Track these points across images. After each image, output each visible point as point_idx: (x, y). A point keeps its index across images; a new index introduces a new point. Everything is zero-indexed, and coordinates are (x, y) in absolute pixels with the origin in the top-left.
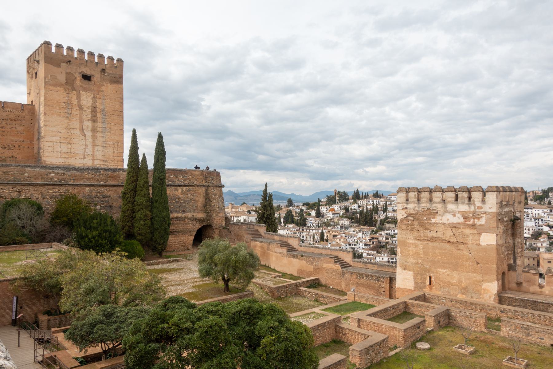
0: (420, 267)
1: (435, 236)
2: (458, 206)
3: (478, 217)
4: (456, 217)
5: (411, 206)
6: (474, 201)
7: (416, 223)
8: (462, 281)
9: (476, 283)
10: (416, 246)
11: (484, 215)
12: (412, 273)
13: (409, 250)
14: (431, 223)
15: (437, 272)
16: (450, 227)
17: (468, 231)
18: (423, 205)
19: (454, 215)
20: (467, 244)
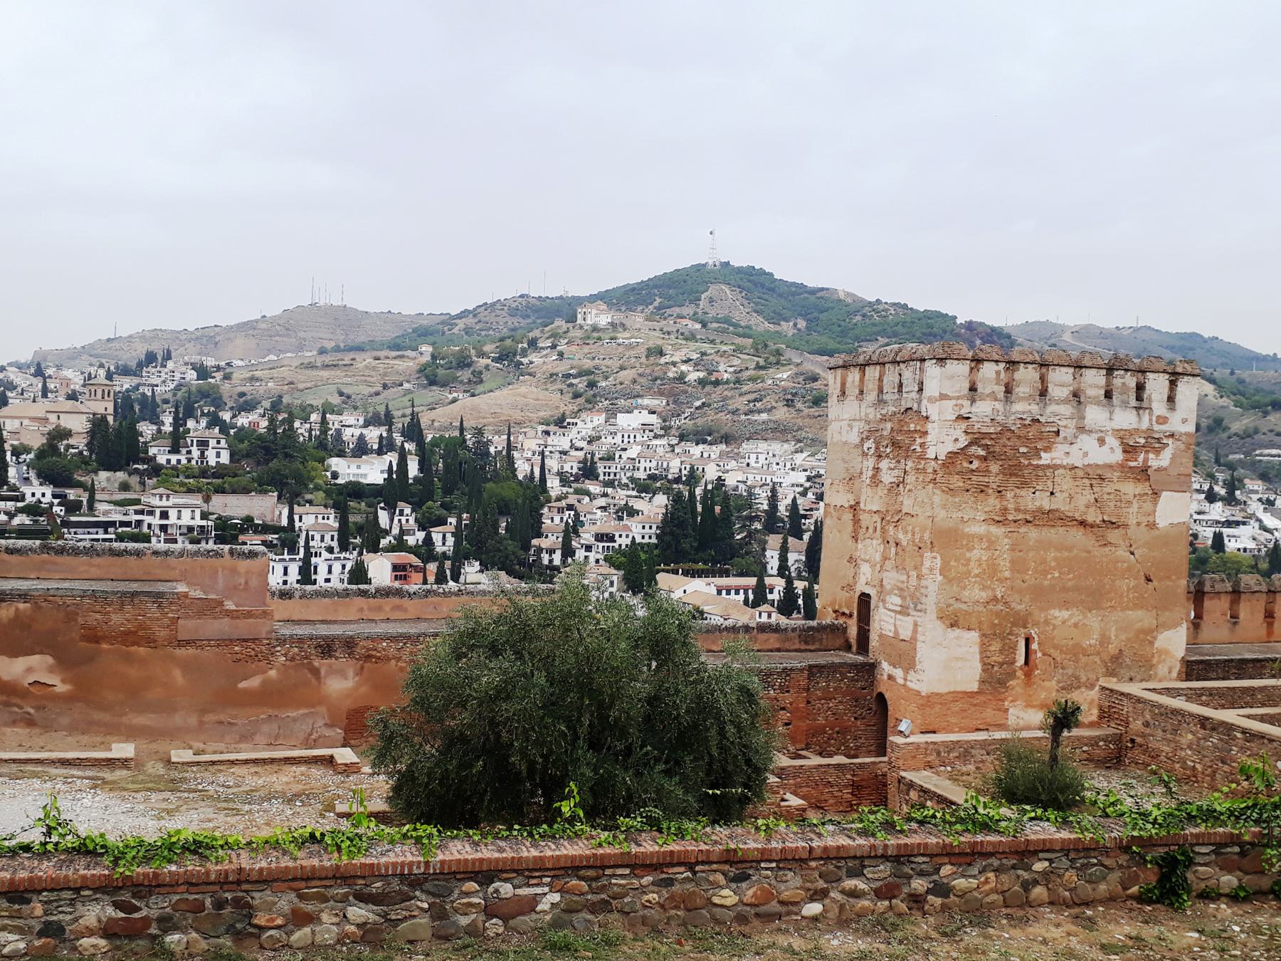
0: (998, 614)
1: (1047, 508)
2: (1111, 413)
3: (1157, 445)
4: (1106, 447)
5: (983, 410)
6: (1150, 400)
7: (994, 467)
8: (1110, 638)
9: (1141, 636)
10: (991, 544)
11: (1170, 441)
12: (974, 636)
13: (969, 560)
14: (1038, 466)
15: (1047, 622)
16: (1088, 477)
17: (1130, 489)
18: (1019, 407)
19: (1102, 441)
20: (1126, 526)
